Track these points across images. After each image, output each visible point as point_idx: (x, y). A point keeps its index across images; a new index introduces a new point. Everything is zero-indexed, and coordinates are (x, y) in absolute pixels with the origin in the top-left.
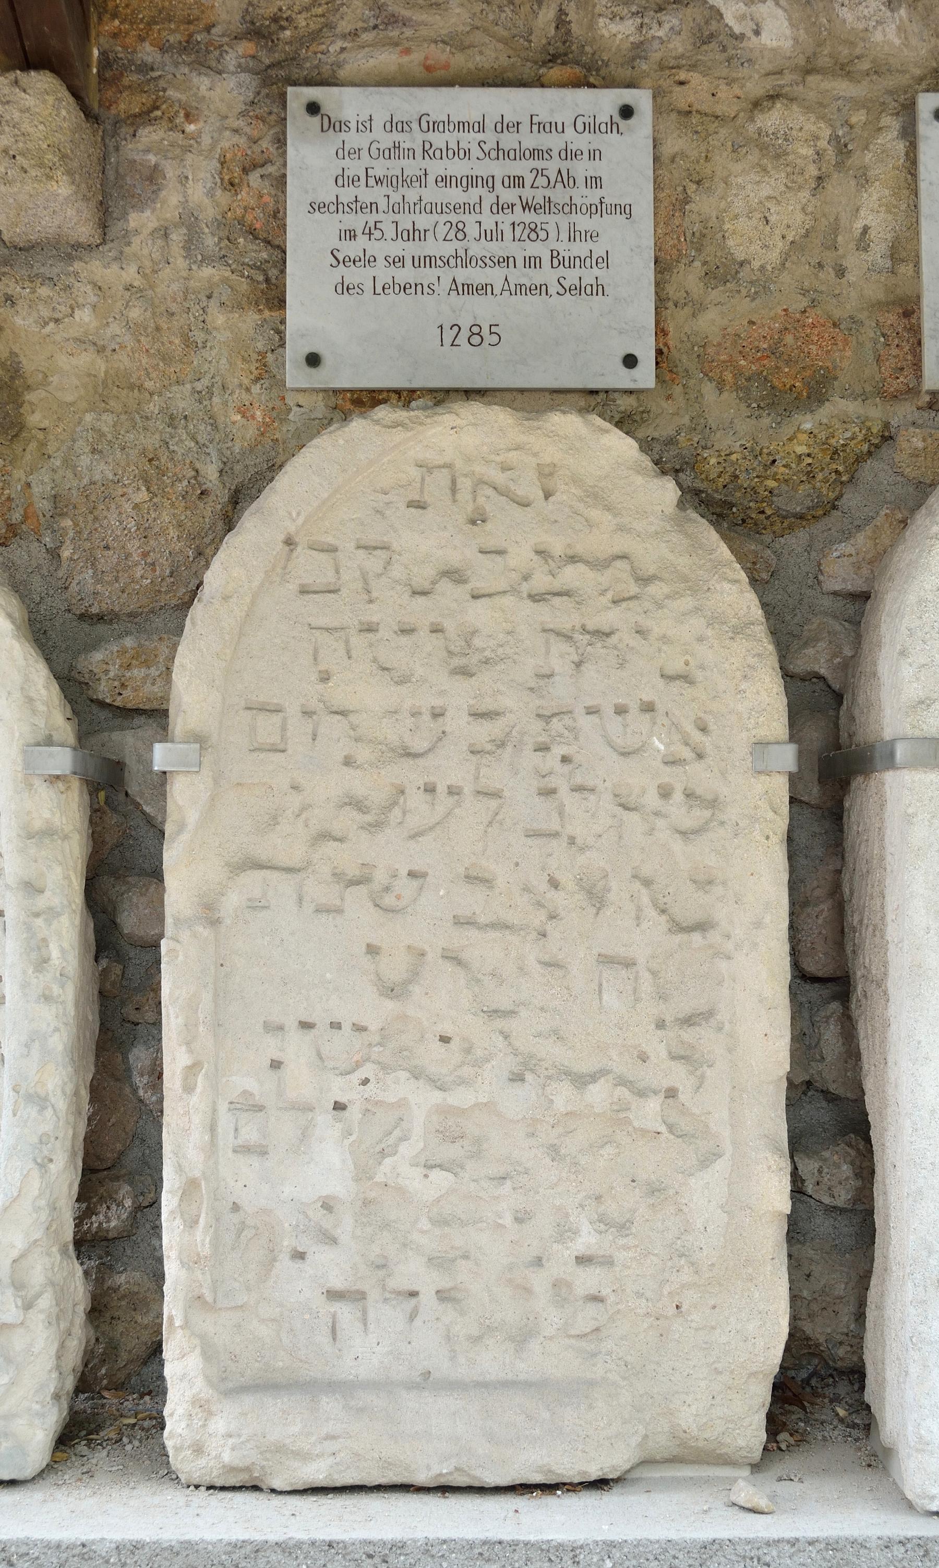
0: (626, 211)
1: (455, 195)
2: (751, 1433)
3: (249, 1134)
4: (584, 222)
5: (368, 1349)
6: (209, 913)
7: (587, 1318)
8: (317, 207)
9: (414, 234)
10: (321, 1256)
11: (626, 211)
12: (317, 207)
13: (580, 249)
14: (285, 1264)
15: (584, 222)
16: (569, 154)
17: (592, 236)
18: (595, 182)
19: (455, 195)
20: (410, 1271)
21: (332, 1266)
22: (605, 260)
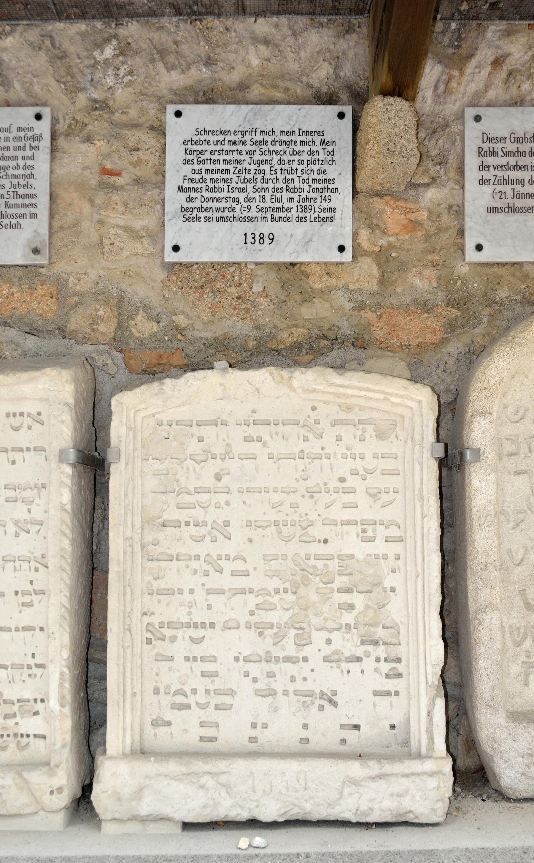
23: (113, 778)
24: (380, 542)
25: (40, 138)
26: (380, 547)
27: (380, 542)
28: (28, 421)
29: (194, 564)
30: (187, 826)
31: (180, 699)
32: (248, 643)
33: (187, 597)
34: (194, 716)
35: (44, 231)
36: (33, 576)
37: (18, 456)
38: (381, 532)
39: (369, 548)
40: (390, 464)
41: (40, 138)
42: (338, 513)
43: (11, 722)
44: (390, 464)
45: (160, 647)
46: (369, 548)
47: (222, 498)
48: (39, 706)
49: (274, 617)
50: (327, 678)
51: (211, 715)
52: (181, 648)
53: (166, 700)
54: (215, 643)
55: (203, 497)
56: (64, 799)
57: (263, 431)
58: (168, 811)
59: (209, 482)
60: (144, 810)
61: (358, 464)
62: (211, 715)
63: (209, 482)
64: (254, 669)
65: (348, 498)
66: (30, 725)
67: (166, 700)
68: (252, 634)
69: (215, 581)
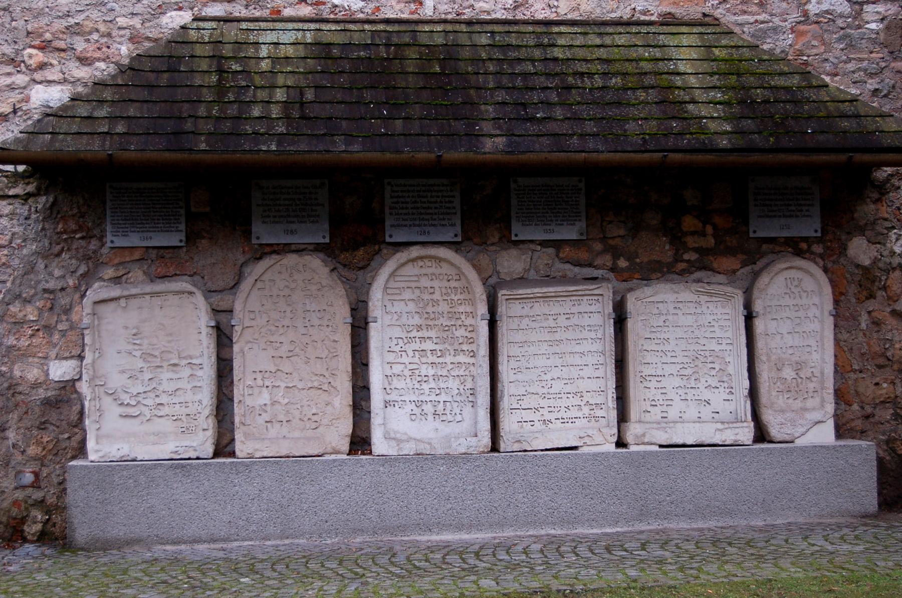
0: (323, 205)
1: (287, 202)
2: (346, 447)
3: (250, 392)
4: (314, 208)
5: (273, 431)
6: (242, 351)
7: (314, 425)
8: (258, 205)
9: (279, 211)
10: (264, 415)
11: (323, 205)
12: (258, 205)
13: (314, 213)
14: (257, 417)
15: (314, 208)
16: (310, 193)
17: (316, 211)
18: (316, 199)
19: (287, 202)
20: (281, 417)
21: (265, 416)
22: (318, 216)
23: (633, 431)
24: (724, 344)
25: (581, 189)
26: (723, 347)
27: (724, 344)
28: (594, 302)
29: (657, 354)
30: (661, 446)
31: (653, 403)
32: (677, 382)
33: (655, 366)
34: (657, 410)
35: (585, 226)
36: (599, 358)
37: (591, 315)
38: (725, 342)
39: (721, 347)
40: (727, 317)
41: (581, 189)
42: (708, 335)
43: (592, 412)
44: (727, 317)
45: (646, 384)
46: (721, 347)
47: (666, 329)
48: (603, 406)
49: (686, 372)
50: (706, 395)
51: (665, 408)
52: (653, 384)
53: (648, 403)
54: (665, 382)
55: (659, 329)
56: (615, 439)
57: (680, 305)
58: (654, 440)
59: (661, 324)
60: (646, 440)
61: (715, 317)
62: (665, 408)
63: (661, 324)
64: (680, 392)
65: (712, 329)
66: (600, 413)
67: (648, 403)
68: (679, 379)
69: (664, 360)
